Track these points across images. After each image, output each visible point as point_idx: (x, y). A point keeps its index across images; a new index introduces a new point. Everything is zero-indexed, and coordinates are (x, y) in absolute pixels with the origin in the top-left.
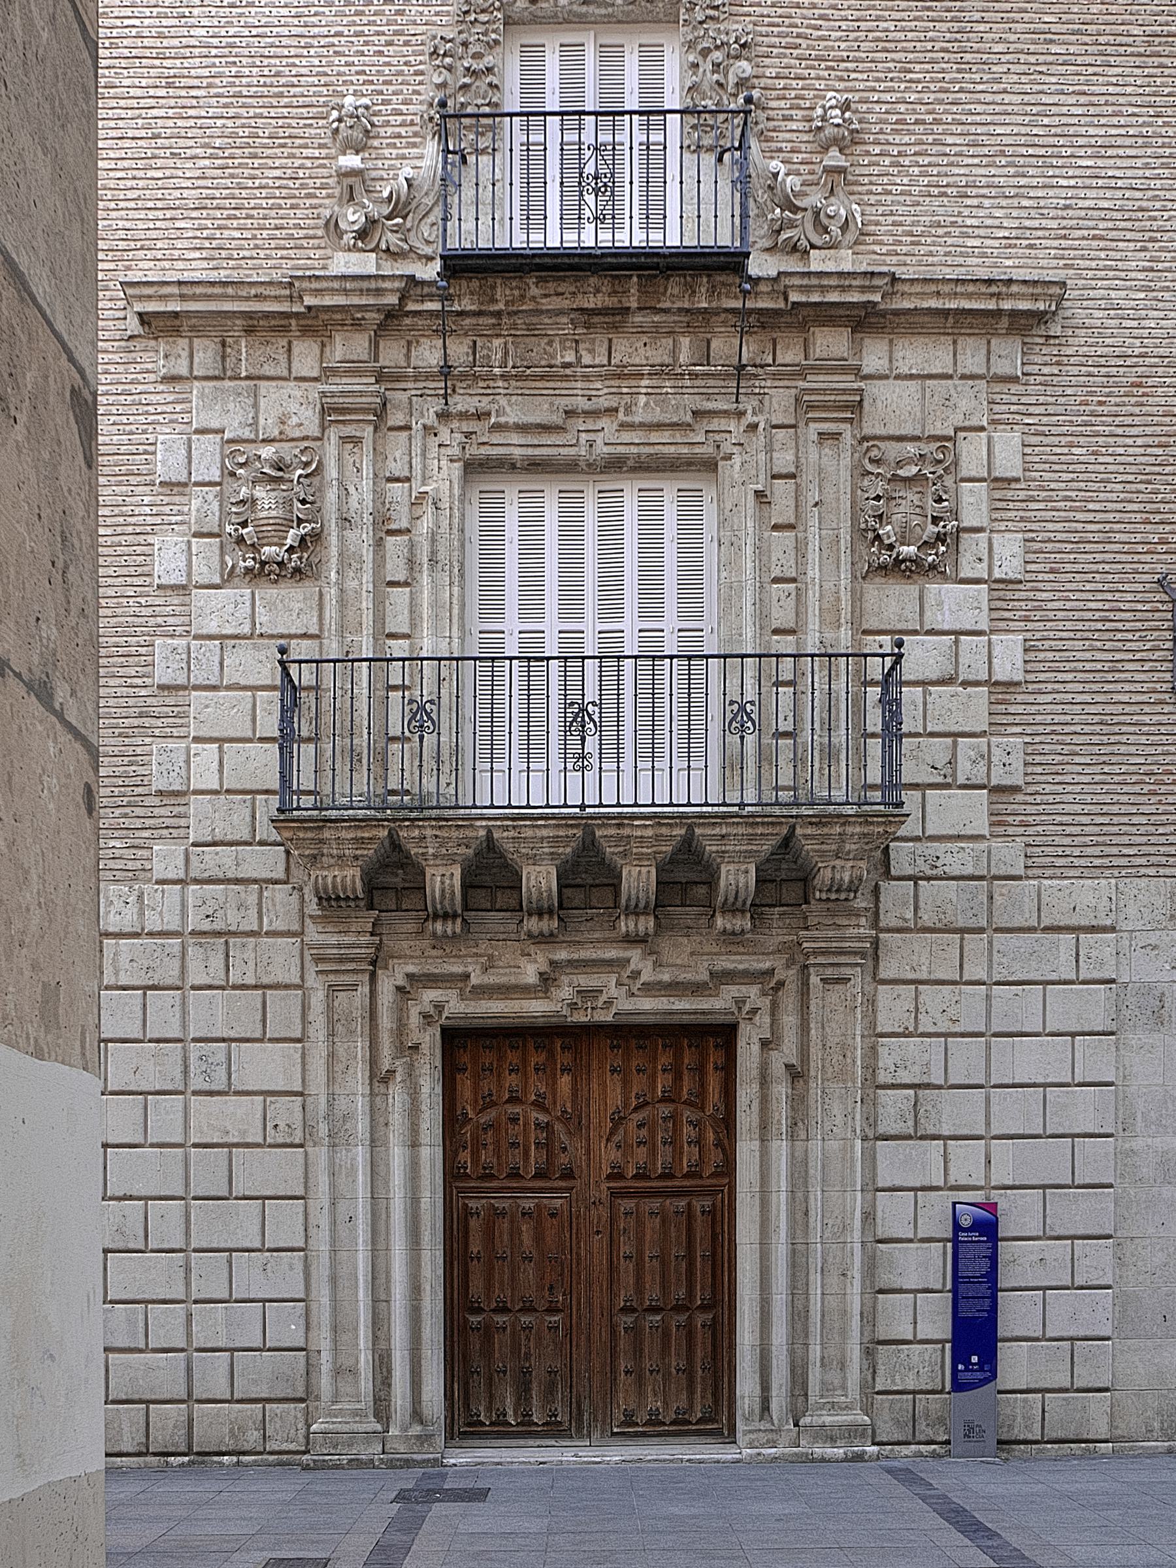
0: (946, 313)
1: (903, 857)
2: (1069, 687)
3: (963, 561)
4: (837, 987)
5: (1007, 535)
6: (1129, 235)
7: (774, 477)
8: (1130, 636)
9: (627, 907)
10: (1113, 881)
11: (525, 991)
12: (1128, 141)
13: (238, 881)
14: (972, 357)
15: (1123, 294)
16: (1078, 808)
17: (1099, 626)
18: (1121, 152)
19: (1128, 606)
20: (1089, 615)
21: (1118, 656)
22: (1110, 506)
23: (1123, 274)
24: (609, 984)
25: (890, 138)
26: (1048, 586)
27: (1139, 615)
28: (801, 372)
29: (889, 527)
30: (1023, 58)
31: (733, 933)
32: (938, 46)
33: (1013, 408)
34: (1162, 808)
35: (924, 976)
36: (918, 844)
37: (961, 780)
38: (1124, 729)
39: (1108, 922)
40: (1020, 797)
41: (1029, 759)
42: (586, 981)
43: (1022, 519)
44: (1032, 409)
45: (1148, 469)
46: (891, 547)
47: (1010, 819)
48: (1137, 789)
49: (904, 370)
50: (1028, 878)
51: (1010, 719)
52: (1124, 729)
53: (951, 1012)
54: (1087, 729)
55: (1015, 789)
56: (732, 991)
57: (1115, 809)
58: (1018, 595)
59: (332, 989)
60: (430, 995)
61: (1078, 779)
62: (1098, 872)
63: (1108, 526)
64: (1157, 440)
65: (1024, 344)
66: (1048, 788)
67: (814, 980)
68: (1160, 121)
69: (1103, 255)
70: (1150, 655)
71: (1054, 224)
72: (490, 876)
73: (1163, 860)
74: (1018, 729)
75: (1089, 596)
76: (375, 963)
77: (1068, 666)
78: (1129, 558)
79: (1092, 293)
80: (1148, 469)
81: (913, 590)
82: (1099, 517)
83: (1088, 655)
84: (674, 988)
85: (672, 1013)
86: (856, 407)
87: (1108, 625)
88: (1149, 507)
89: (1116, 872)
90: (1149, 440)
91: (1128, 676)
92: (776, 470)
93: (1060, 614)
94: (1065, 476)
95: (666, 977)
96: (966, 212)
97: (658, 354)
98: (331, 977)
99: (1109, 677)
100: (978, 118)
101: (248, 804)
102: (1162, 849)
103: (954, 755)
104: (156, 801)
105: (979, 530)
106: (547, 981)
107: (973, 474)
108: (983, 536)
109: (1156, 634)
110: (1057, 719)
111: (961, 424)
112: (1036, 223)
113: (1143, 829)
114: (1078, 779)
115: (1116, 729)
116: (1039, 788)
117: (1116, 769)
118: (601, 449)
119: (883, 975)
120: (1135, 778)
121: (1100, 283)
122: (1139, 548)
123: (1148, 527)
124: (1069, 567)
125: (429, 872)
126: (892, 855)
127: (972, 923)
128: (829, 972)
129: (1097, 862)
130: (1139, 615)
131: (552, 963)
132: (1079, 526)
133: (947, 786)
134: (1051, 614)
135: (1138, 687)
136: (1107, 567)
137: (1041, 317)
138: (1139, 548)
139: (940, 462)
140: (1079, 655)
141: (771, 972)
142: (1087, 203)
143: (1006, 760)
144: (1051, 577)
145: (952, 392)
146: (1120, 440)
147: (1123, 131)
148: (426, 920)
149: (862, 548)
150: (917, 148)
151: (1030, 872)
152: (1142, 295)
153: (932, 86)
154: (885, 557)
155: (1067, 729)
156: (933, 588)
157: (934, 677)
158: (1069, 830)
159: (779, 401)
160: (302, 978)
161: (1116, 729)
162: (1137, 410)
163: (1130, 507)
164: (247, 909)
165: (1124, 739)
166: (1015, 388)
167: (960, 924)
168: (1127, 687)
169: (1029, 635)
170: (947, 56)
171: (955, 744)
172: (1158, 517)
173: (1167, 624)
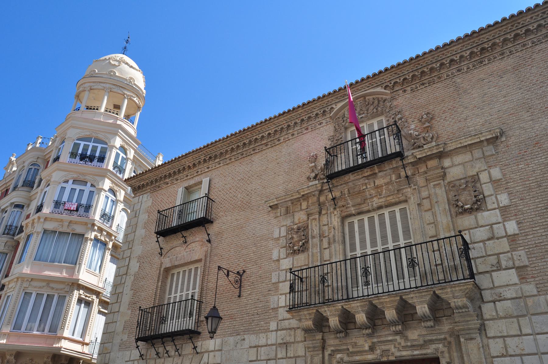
0: (466, 146)
3: (488, 205)
35: (505, 334)
37: (504, 267)
40: (529, 269)
46: (462, 207)
49: (457, 163)
59: (312, 357)
60: (339, 356)
67: (462, 340)
74: (522, 248)
81: (473, 217)
95: (409, 344)
98: (312, 353)
105: (492, 195)
106: (372, 349)
107: (485, 181)
118: (375, 206)
128: (467, 336)
131: (373, 343)
141: (445, 339)
143: (519, 258)
151: (541, 293)
154: (460, 210)
156: (479, 215)
157: (486, 238)
160: (305, 354)
169: (518, 220)
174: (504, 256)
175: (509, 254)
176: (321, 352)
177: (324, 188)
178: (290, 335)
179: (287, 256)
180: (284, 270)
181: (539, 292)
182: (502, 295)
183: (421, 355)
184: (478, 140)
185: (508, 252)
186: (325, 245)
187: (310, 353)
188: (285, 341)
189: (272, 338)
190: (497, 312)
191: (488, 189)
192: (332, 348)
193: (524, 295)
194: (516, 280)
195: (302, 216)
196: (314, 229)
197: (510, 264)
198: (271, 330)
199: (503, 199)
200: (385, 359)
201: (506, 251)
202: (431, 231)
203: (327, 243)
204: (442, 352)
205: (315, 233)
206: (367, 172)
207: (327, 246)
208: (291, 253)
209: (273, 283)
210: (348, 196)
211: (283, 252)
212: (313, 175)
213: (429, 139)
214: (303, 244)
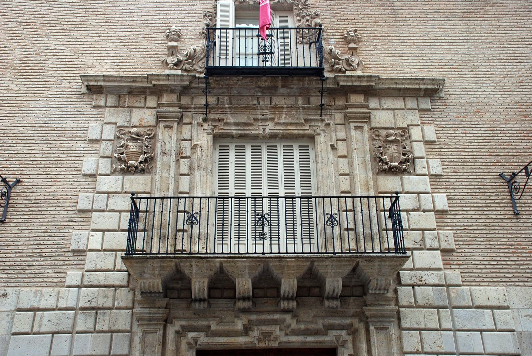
1: (405, 276)
2: (469, 212)
4: (383, 331)
5: (434, 160)
6: (466, 67)
7: (337, 140)
8: (491, 194)
9: (284, 296)
10: (504, 287)
11: (237, 334)
12: (460, 41)
13: (105, 286)
14: (411, 103)
15: (467, 84)
16: (481, 258)
17: (478, 191)
18: (458, 44)
19: (488, 184)
20: (472, 187)
21: (488, 201)
22: (474, 150)
23: (466, 79)
24: (276, 330)
25: (372, 41)
26: (454, 177)
27: (494, 187)
28: (346, 107)
29: (386, 157)
30: (418, 19)
31: (333, 308)
32: (386, 16)
33: (430, 119)
34: (520, 259)
35: (423, 326)
36: (412, 272)
38: (496, 228)
39: (506, 305)
40: (455, 254)
41: (456, 239)
42: (265, 328)
43: (439, 155)
44: (437, 119)
45: (487, 138)
47: (452, 262)
48: (507, 251)
50: (464, 285)
51: (446, 224)
52: (496, 228)
53: (438, 343)
54: (479, 228)
55: (452, 251)
56: (334, 333)
57: (498, 258)
58: (441, 180)
59: (145, 333)
60: (191, 335)
61: (479, 247)
62: (496, 284)
63: (475, 157)
64: (489, 129)
65: (431, 99)
66: (467, 250)
67: (372, 328)
68: (472, 35)
69: (457, 73)
70: (502, 201)
71: (437, 64)
72: (221, 285)
73: (526, 279)
74: (450, 228)
75: (472, 180)
76: (166, 322)
77: (467, 205)
78: (486, 167)
79: (455, 84)
80: (487, 138)
81: (398, 178)
82: (470, 154)
83: (475, 201)
84: (306, 333)
85: (306, 342)
86: (367, 118)
87: (481, 190)
88: (490, 150)
89: (504, 284)
90: (486, 129)
91: (494, 208)
92: (338, 138)
93: (460, 187)
94: (454, 141)
95: (303, 327)
96: (403, 61)
97: (290, 101)
98: (145, 327)
99: (486, 209)
100: (404, 35)
101: (114, 255)
102: (524, 275)
103: (423, 237)
104: (71, 254)
106: (247, 330)
107: (417, 139)
108: (424, 160)
109: (502, 194)
110: (466, 224)
111: (410, 124)
112: (430, 64)
113: (513, 267)
114: (479, 247)
115: (493, 228)
116: (463, 250)
117: (496, 243)
119: (404, 325)
120: (505, 247)
121: (457, 81)
122: (489, 164)
123: (491, 157)
124: (461, 170)
125: (193, 281)
126: (401, 276)
127: (441, 304)
128: (378, 325)
129: (495, 280)
130: (494, 187)
131: (250, 321)
132: (463, 157)
133: (421, 249)
134: (456, 187)
135: (499, 213)
136: (477, 171)
137: (436, 91)
138: (489, 164)
139: (402, 136)
140: (471, 201)
141: (351, 325)
142: (448, 58)
143: (446, 239)
144: (455, 174)
145: (405, 113)
146: (474, 129)
147: (458, 38)
148: (191, 302)
149: (375, 164)
150: (382, 43)
151: (464, 283)
152: (474, 85)
153: (386, 27)
154: (385, 166)
155: (471, 228)
156: (406, 177)
157: (411, 208)
158: (479, 267)
159: (338, 117)
160: (131, 327)
161: (493, 228)
162: (479, 120)
163: (482, 150)
164: (108, 298)
165: (497, 232)
166: (429, 113)
167: (437, 304)
168: (494, 213)
169: (448, 194)
170: (390, 19)
171: (423, 234)
172: (495, 154)
173: (506, 190)
174: (430, 234)
175: (435, 232)
176: (162, 327)
177: (193, 85)
178: (105, 296)
179: (114, 172)
180: (103, 193)
181: (463, 281)
182: (423, 279)
183: (317, 342)
184: (417, 87)
185: (434, 229)
186: (184, 169)
187: (141, 328)
188: (94, 305)
189: (69, 298)
190: (415, 298)
191: (419, 150)
192: (183, 323)
193: (448, 283)
194: (440, 264)
195: (145, 116)
196: (167, 139)
197: (436, 244)
198: (67, 283)
199: (435, 166)
200: (262, 345)
201: (432, 227)
202: (345, 185)
203: (186, 167)
204: (345, 342)
205: (168, 147)
206: (266, 81)
207: (186, 172)
208: (122, 169)
209: (81, 211)
210: (229, 108)
211: (105, 166)
212: (172, 60)
213: (355, 65)
214: (146, 160)
